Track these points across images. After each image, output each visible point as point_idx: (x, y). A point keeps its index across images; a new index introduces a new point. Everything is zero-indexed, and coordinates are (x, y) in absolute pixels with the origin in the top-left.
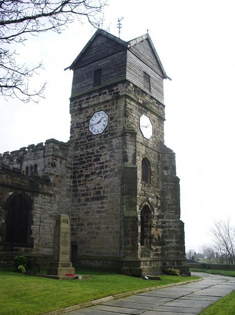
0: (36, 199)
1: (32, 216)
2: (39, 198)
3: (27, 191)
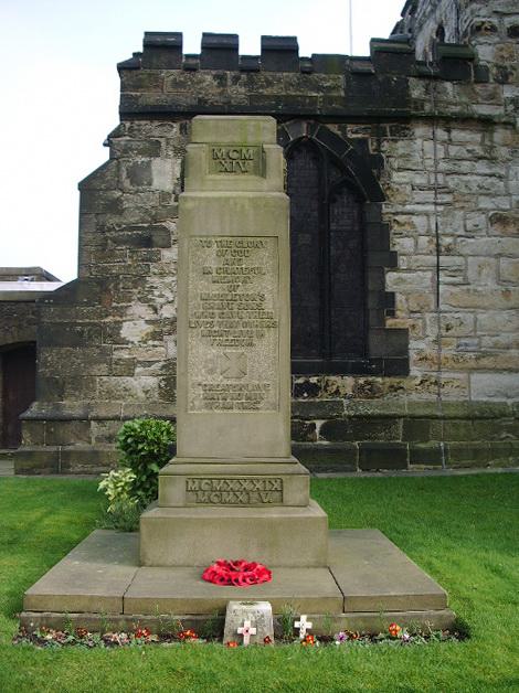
0: (395, 150)
1: (384, 231)
2: (419, 141)
3: (341, 119)
